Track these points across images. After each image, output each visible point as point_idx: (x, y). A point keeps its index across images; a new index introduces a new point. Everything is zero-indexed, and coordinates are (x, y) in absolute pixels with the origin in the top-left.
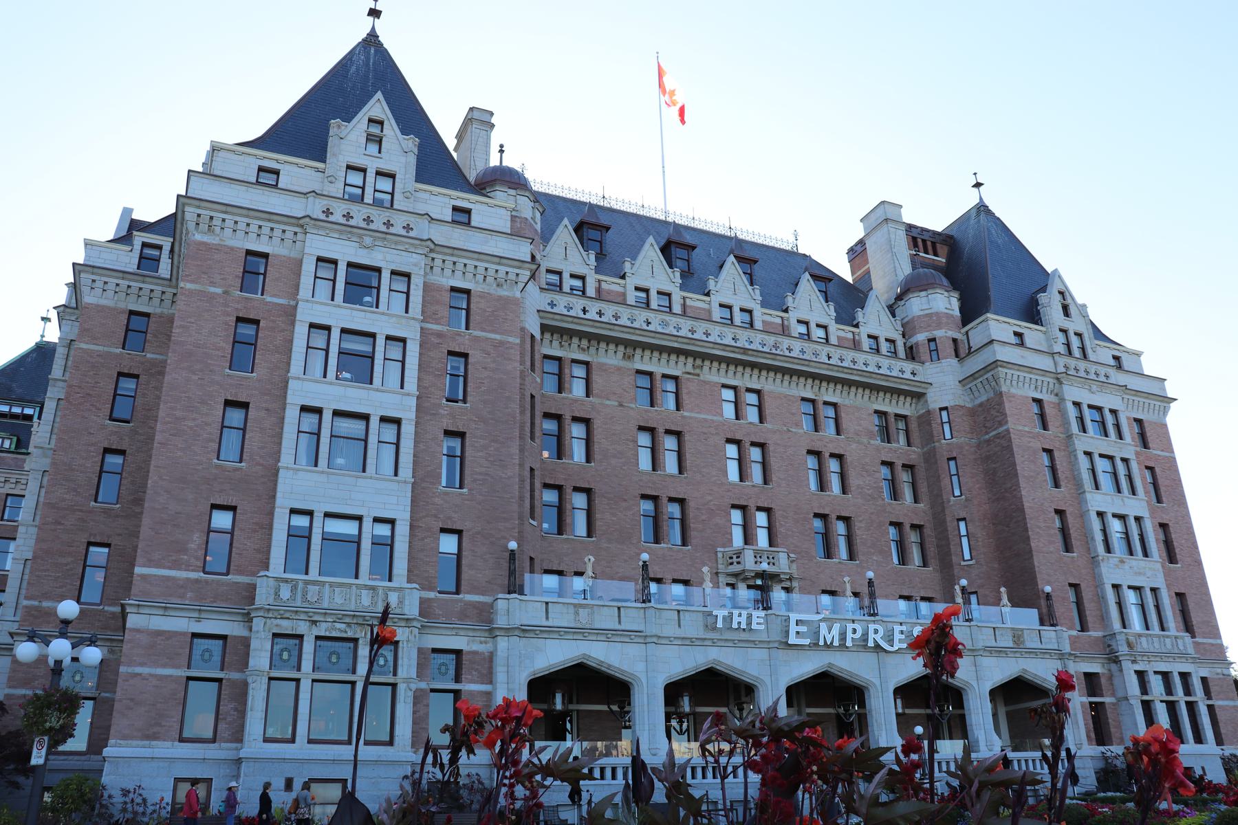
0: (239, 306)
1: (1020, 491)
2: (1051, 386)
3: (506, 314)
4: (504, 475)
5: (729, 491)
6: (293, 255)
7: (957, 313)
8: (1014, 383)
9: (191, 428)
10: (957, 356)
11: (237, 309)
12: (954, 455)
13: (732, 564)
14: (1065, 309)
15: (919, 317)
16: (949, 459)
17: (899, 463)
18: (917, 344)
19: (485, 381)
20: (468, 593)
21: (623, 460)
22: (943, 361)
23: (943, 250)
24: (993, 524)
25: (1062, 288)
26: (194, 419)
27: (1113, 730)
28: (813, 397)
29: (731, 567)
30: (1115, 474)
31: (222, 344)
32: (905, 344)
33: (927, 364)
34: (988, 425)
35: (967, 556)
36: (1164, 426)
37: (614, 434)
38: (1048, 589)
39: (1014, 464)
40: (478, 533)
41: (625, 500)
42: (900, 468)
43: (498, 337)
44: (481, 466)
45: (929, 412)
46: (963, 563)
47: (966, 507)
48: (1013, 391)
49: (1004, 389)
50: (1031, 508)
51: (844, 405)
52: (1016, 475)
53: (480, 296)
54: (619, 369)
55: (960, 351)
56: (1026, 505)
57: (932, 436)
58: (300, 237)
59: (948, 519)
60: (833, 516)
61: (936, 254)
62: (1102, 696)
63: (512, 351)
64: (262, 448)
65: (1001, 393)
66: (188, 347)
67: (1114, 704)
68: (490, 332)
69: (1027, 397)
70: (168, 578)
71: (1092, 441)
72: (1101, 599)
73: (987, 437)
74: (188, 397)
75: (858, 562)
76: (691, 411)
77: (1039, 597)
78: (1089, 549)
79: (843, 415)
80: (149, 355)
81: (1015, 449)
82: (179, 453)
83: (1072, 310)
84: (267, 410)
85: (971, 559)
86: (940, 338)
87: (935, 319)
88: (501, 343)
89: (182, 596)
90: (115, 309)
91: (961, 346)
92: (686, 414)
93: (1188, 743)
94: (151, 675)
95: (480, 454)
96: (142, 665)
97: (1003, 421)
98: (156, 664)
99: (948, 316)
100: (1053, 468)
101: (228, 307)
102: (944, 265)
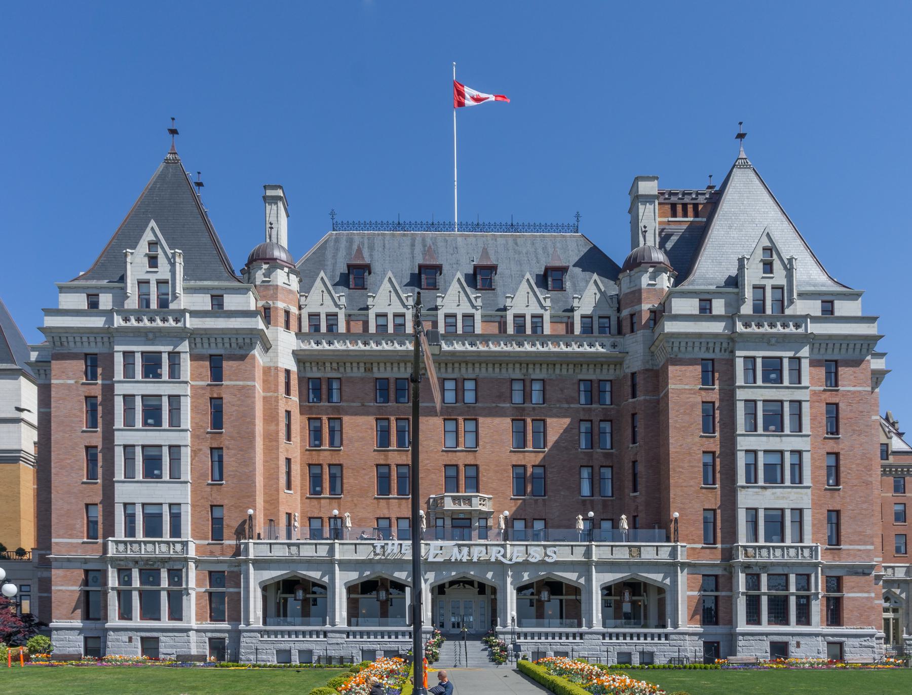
3: (246, 367)
4: (247, 471)
9: (68, 464)
19: (234, 413)
21: (363, 443)
28: (522, 377)
33: (627, 335)
37: (358, 426)
41: (364, 469)
43: (241, 383)
44: (233, 467)
68: (236, 380)
70: (68, 543)
74: (65, 447)
82: (65, 479)
88: (243, 387)
89: (76, 552)
94: (67, 590)
95: (233, 459)
96: (62, 585)
98: (68, 585)
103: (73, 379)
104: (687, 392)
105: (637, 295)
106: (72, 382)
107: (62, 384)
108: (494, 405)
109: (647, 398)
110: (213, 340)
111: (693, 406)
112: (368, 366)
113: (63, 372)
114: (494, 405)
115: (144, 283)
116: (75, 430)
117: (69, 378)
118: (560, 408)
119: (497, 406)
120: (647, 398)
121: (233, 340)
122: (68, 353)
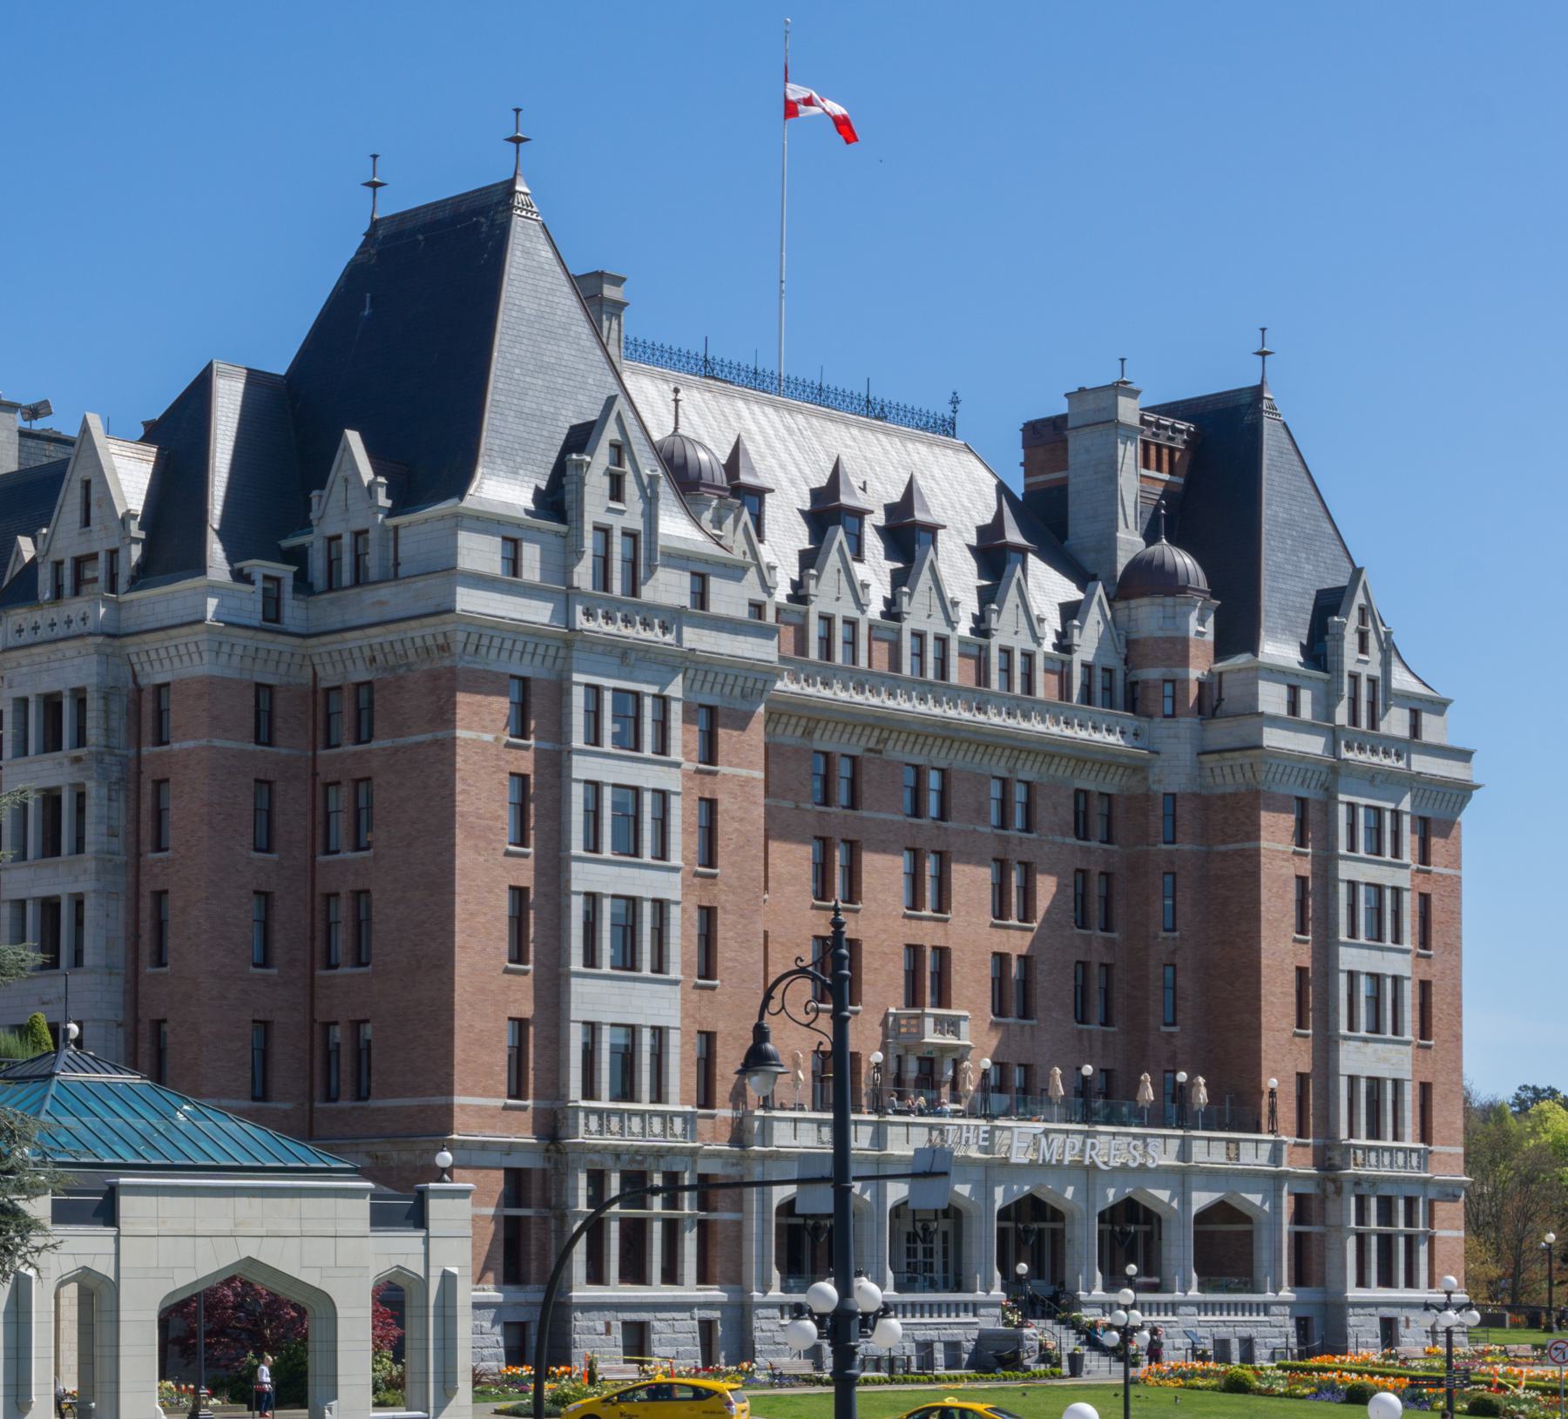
1: (1259, 943)
2: (1323, 778)
8: (1278, 776)
15: (1157, 640)
16: (1165, 873)
17: (1095, 870)
18: (1146, 682)
28: (1006, 775)
31: (501, 812)
32: (1126, 675)
33: (1157, 719)
38: (1273, 1082)
40: (730, 1034)
42: (1096, 878)
48: (1274, 789)
56: (1264, 961)
58: (562, 653)
62: (1309, 1224)
69: (1289, 797)
73: (1222, 848)
75: (1034, 1022)
77: (1261, 1093)
79: (1039, 800)
80: (283, 751)
92: (865, 814)
103: (491, 732)
104: (1280, 855)
105: (1179, 647)
107: (474, 740)
110: (710, 677)
112: (811, 725)
113: (476, 714)
114: (971, 827)
115: (604, 531)
117: (484, 729)
119: (975, 830)
120: (1195, 847)
121: (740, 682)
122: (485, 671)
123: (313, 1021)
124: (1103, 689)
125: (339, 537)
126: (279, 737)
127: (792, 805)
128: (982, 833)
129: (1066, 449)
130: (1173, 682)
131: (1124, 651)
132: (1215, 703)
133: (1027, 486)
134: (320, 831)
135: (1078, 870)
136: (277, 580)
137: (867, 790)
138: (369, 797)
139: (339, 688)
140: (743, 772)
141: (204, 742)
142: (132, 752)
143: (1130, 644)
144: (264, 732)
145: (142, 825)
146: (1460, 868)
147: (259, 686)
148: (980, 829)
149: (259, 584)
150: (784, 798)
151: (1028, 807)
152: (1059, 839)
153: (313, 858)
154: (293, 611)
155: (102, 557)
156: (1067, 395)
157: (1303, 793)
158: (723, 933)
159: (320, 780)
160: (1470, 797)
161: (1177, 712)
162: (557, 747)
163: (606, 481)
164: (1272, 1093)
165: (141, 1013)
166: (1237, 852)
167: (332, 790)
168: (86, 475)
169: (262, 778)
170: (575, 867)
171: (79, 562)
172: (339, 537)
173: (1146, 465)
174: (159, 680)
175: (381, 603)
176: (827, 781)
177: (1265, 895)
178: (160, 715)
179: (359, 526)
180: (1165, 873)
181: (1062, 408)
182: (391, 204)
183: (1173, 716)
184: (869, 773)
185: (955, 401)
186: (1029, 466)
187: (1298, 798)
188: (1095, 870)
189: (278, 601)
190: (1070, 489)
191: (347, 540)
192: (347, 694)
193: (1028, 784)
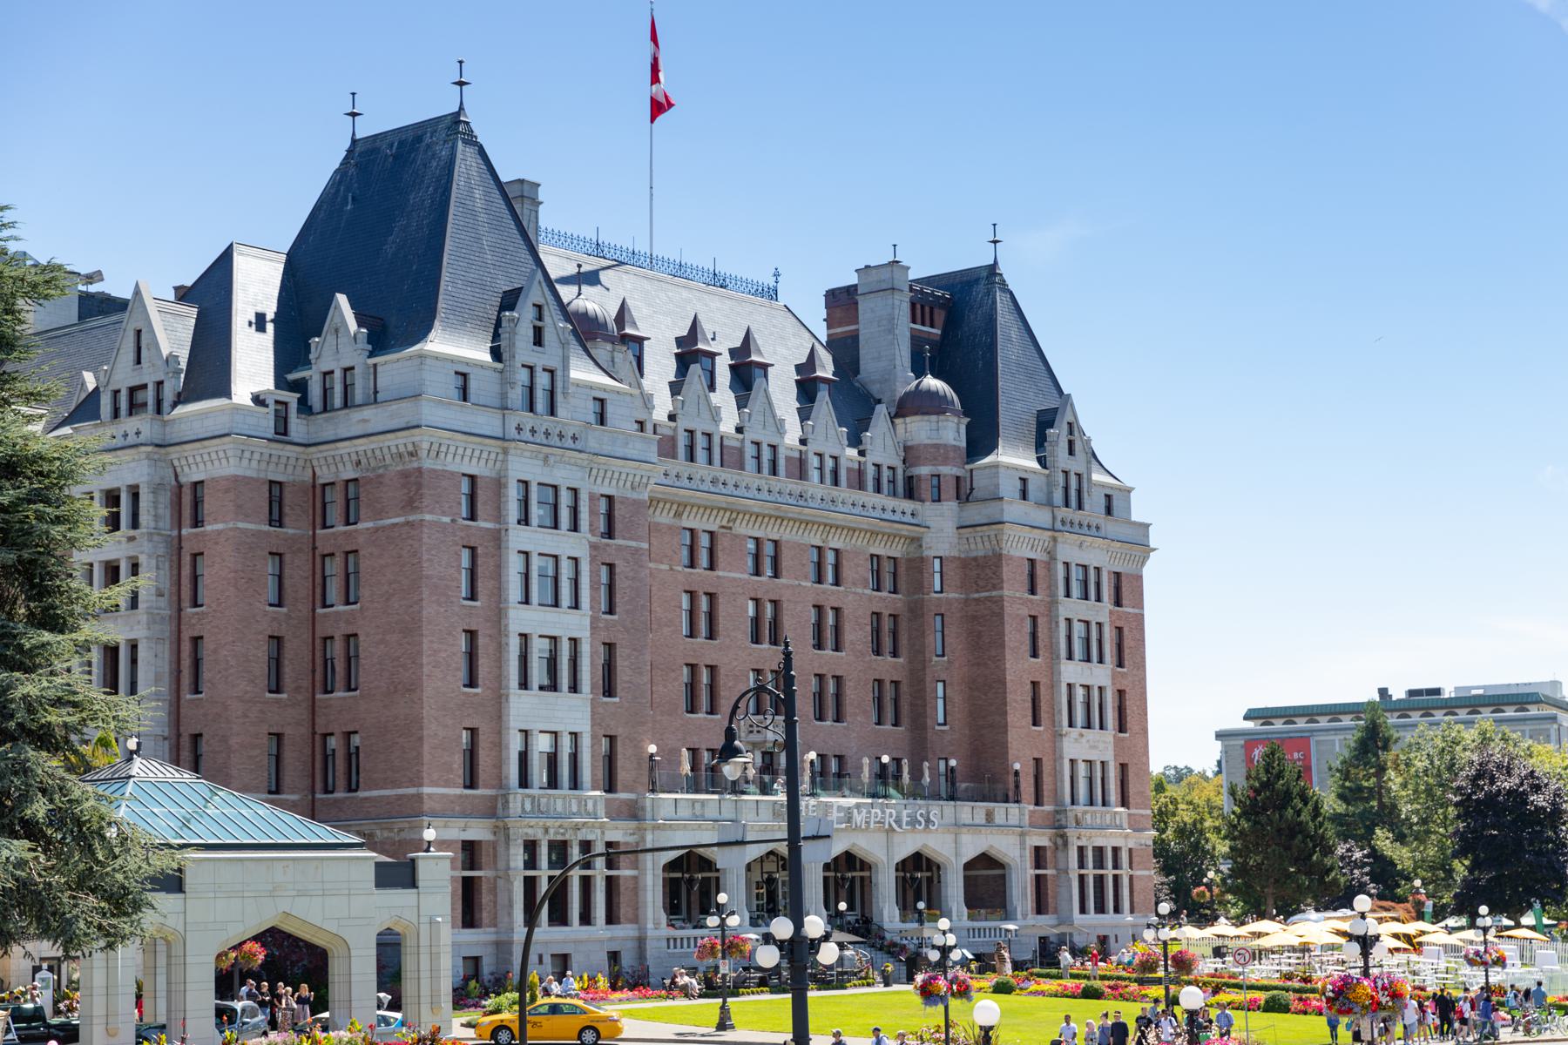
0: (462, 534)
1: (1005, 664)
2: (1046, 544)
5: (750, 655)
6: (494, 475)
7: (964, 444)
8: (1014, 544)
9: (444, 658)
10: (958, 499)
11: (462, 538)
12: (943, 611)
13: (751, 732)
14: (1071, 443)
16: (936, 615)
17: (886, 613)
18: (919, 477)
20: (623, 792)
22: (945, 503)
23: (940, 316)
24: (970, 688)
25: (1069, 418)
26: (446, 651)
27: (1050, 900)
28: (820, 544)
29: (751, 735)
30: (1087, 640)
32: (904, 471)
33: (928, 503)
34: (981, 583)
35: (941, 720)
36: (1140, 578)
38: (1017, 766)
39: (1002, 634)
40: (627, 737)
42: (887, 619)
45: (922, 559)
46: (937, 728)
47: (947, 669)
49: (1004, 552)
50: (1012, 681)
51: (847, 551)
52: (1003, 646)
53: (622, 503)
54: (670, 528)
55: (964, 492)
56: (1008, 678)
57: (922, 587)
59: (928, 679)
60: (829, 676)
61: (932, 326)
62: (1045, 868)
63: (643, 558)
64: (489, 673)
65: (1001, 555)
66: (435, 580)
67: (1054, 876)
69: (1023, 558)
71: (1072, 608)
72: (1057, 774)
73: (976, 596)
75: (845, 724)
76: (724, 570)
77: (1008, 773)
78: (1054, 721)
80: (291, 531)
81: (1006, 618)
83: (1078, 447)
84: (490, 636)
85: (945, 724)
86: (945, 476)
87: (939, 452)
90: (256, 480)
91: (962, 484)
92: (720, 573)
93: (1108, 913)
97: (998, 586)
99: (956, 448)
100: (1034, 636)
101: (455, 536)
102: (938, 338)
105: (942, 451)
106: (447, 520)
108: (797, 582)
109: (957, 595)
110: (609, 474)
111: (1022, 620)
113: (437, 502)
114: (797, 582)
116: (451, 602)
117: (444, 514)
118: (855, 593)
120: (957, 595)
123: (314, 733)
124: (889, 481)
125: (332, 372)
126: (286, 520)
127: (667, 567)
128: (805, 587)
129: (857, 309)
130: (939, 476)
131: (903, 454)
132: (968, 491)
133: (829, 336)
134: (318, 591)
135: (873, 613)
136: (285, 404)
137: (721, 557)
138: (356, 564)
139: (332, 484)
140: (633, 544)
141: (231, 525)
142: (175, 533)
143: (907, 449)
144: (276, 519)
145: (183, 588)
146: (1143, 608)
147: (271, 482)
148: (803, 584)
149: (272, 407)
150: (662, 563)
151: (837, 567)
152: (859, 590)
153: (314, 610)
154: (298, 428)
155: (151, 387)
156: (856, 271)
157: (1032, 556)
158: (621, 664)
159: (318, 552)
160: (1148, 557)
161: (942, 498)
162: (497, 526)
163: (531, 333)
164: (1017, 773)
165: (182, 729)
166: (986, 598)
167: (327, 560)
168: (139, 326)
169: (275, 551)
170: (512, 614)
171: (133, 391)
172: (332, 372)
173: (914, 321)
174: (196, 478)
175: (365, 421)
176: (692, 550)
177: (1007, 628)
178: (197, 503)
179: (348, 364)
180: (936, 615)
181: (853, 279)
182: (365, 129)
183: (939, 501)
184: (723, 544)
185: (777, 275)
186: (830, 320)
187: (1028, 559)
188: (886, 613)
189: (286, 420)
190: (861, 338)
191: (338, 375)
192: (339, 488)
193: (837, 551)
